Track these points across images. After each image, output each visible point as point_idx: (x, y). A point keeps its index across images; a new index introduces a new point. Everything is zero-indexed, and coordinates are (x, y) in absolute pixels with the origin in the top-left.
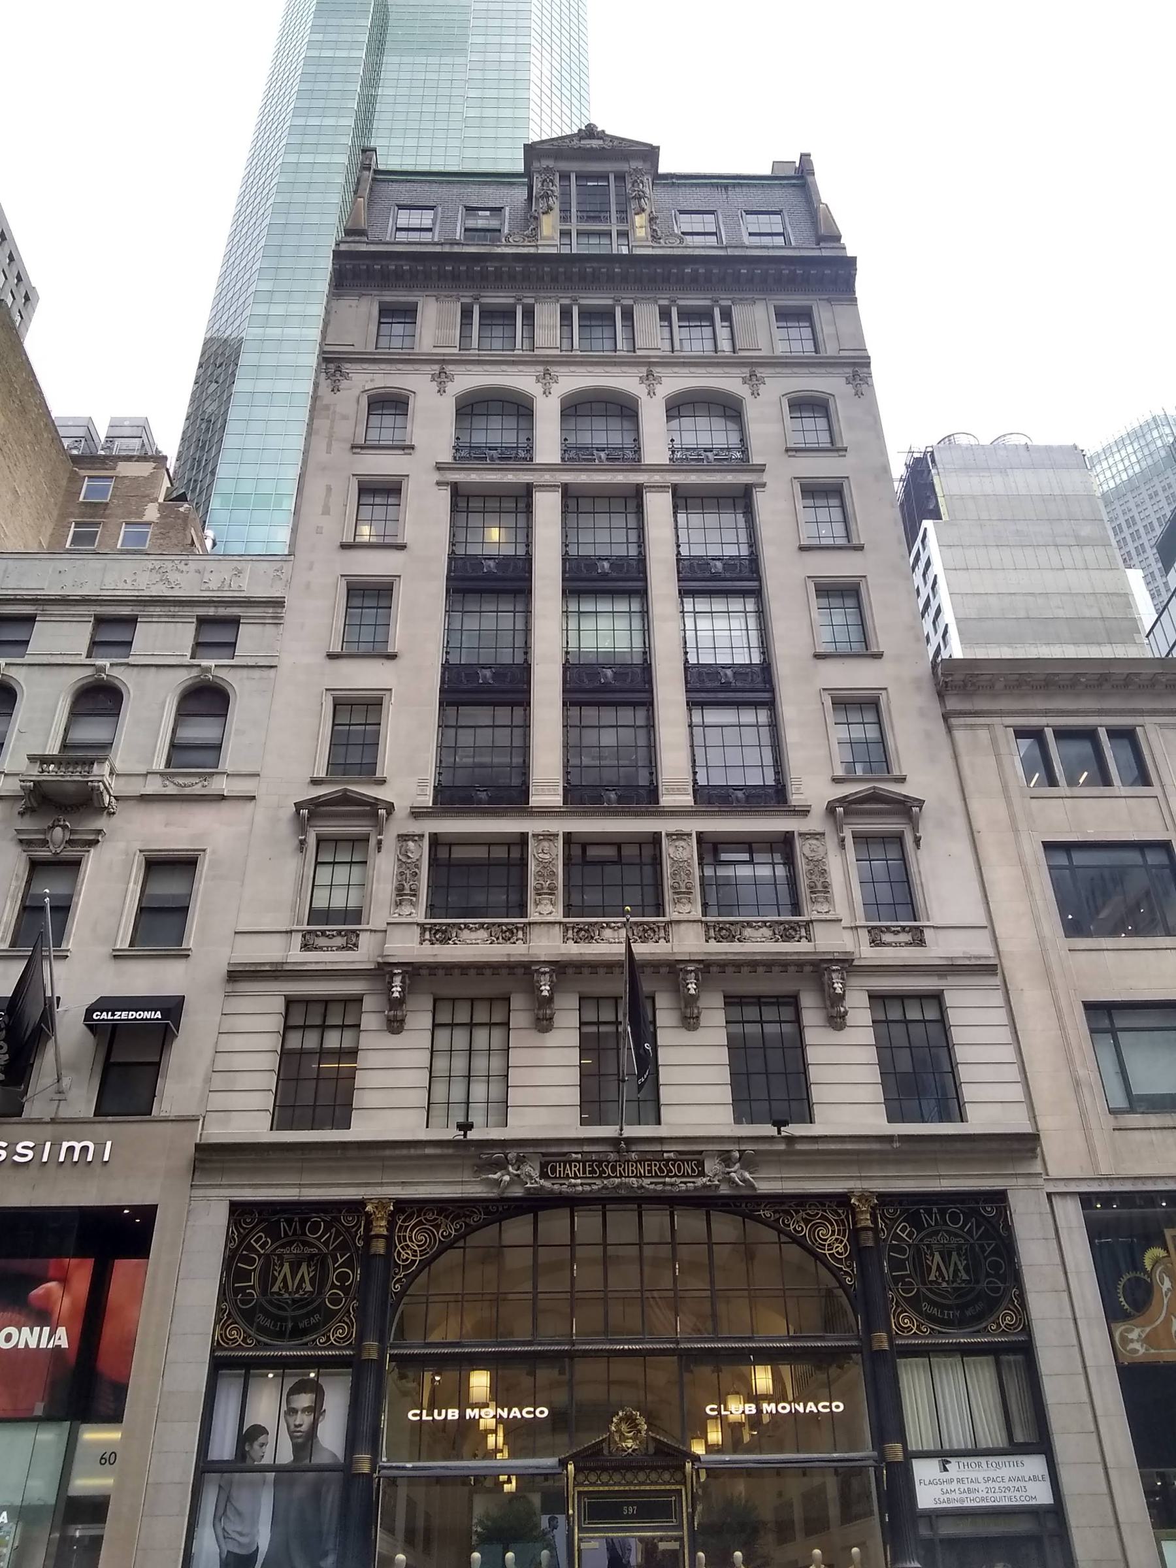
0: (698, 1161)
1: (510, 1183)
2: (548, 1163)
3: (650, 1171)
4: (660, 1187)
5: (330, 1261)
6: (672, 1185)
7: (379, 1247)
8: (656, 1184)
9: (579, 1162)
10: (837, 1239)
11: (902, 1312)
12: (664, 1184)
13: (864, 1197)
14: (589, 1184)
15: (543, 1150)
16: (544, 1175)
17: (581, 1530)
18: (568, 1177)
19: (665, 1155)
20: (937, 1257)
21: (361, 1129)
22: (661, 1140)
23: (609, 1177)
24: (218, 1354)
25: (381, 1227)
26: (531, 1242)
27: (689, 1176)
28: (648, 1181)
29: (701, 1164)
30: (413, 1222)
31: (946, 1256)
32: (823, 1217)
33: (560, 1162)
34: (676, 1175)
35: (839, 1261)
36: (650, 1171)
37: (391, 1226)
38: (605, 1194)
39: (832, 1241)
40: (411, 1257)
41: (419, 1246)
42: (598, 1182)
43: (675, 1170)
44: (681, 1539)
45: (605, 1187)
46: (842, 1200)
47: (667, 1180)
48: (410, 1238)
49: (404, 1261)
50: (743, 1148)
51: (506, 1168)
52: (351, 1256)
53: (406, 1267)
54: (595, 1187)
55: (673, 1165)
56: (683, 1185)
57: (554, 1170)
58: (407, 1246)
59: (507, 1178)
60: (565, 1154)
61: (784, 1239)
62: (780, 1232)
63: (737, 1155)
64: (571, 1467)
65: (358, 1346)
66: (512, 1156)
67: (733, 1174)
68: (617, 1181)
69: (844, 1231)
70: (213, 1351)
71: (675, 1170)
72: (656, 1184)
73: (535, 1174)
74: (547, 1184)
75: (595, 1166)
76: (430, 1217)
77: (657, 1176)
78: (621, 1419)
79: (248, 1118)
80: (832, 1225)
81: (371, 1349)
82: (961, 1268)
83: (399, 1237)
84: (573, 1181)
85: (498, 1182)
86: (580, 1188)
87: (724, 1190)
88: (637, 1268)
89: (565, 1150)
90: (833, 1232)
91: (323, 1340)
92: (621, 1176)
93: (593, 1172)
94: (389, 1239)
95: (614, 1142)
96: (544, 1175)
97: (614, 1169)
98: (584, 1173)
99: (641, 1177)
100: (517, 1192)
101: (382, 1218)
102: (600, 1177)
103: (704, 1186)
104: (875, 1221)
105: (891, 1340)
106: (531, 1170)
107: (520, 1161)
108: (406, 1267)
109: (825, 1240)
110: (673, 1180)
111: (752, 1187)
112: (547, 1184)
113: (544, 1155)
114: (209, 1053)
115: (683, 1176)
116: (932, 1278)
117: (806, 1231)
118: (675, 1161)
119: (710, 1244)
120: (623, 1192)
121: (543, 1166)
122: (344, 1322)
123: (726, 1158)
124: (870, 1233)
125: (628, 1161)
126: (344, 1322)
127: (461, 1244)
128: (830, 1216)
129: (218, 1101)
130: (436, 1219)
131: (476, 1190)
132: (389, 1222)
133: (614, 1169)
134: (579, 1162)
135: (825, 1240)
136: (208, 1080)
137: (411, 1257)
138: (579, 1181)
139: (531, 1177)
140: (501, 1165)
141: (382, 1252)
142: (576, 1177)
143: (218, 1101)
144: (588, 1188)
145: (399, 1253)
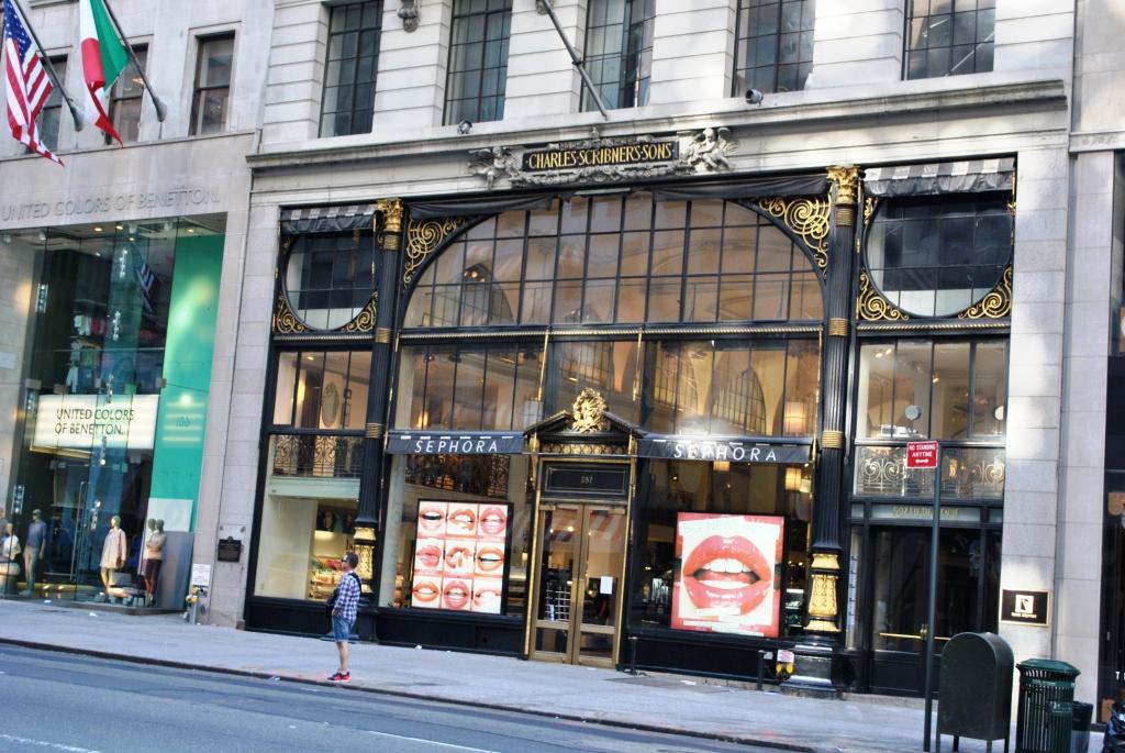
0: (673, 143)
2: (530, 154)
3: (624, 157)
4: (632, 174)
6: (644, 169)
8: (630, 169)
9: (557, 151)
10: (816, 219)
11: (873, 296)
12: (637, 169)
14: (567, 174)
16: (526, 168)
17: (543, 494)
18: (547, 169)
19: (639, 139)
21: (383, 131)
22: (632, 123)
23: (585, 165)
24: (276, 338)
25: (394, 224)
26: (649, 227)
27: (662, 160)
28: (622, 167)
29: (675, 146)
33: (540, 153)
34: (649, 160)
35: (815, 242)
36: (624, 157)
40: (420, 251)
41: (426, 241)
42: (574, 171)
43: (649, 155)
44: (626, 507)
45: (581, 177)
47: (639, 165)
48: (420, 233)
49: (415, 255)
51: (493, 163)
53: (416, 261)
54: (572, 177)
55: (647, 150)
56: (654, 170)
57: (534, 161)
59: (491, 173)
60: (545, 145)
61: (763, 220)
62: (759, 214)
64: (534, 442)
65: (373, 332)
67: (705, 156)
68: (591, 170)
69: (827, 208)
70: (272, 335)
71: (649, 155)
72: (630, 169)
73: (519, 165)
74: (528, 176)
75: (574, 153)
77: (631, 162)
78: (584, 398)
79: (297, 131)
81: (383, 337)
83: (411, 233)
84: (550, 172)
85: (484, 177)
86: (557, 179)
87: (701, 170)
88: (753, 254)
91: (352, 326)
92: (597, 163)
93: (571, 161)
95: (590, 127)
96: (526, 168)
97: (590, 157)
98: (562, 162)
99: (615, 163)
100: (504, 185)
101: (392, 216)
102: (576, 166)
103: (677, 169)
105: (849, 327)
107: (506, 152)
108: (416, 261)
109: (805, 220)
110: (644, 165)
111: (726, 165)
112: (528, 176)
114: (264, 65)
115: (656, 160)
117: (785, 211)
118: (649, 144)
119: (688, 230)
120: (599, 180)
121: (526, 157)
123: (699, 135)
125: (604, 148)
127: (463, 238)
129: (272, 113)
131: (472, 186)
132: (402, 220)
133: (590, 157)
134: (557, 151)
135: (805, 220)
136: (264, 95)
137: (420, 251)
138: (556, 172)
139: (512, 169)
140: (488, 158)
141: (393, 247)
142: (554, 168)
143: (272, 113)
144: (565, 179)
145: (411, 248)
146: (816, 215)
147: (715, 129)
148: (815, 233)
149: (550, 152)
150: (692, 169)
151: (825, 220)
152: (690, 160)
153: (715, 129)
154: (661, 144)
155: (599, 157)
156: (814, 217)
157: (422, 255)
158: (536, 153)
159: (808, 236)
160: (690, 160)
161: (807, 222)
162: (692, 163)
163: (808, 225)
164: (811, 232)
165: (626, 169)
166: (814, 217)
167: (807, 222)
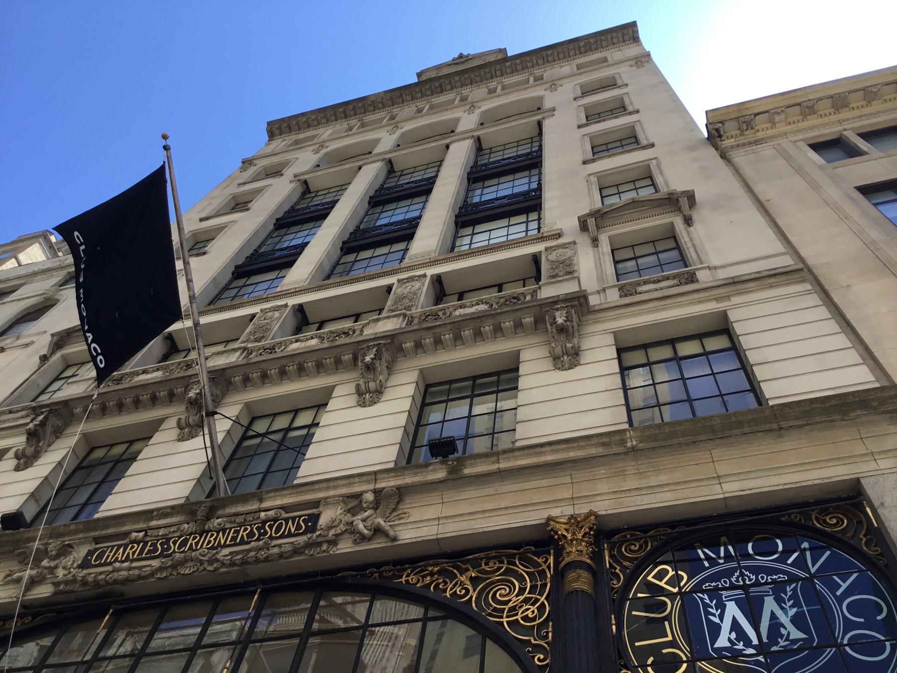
10: (526, 601)
13: (574, 521)
20: (732, 610)
31: (752, 609)
32: (508, 572)
39: (519, 602)
46: (542, 541)
50: (380, 485)
55: (271, 527)
63: (370, 497)
69: (545, 585)
80: (521, 579)
82: (784, 619)
90: (522, 591)
104: (597, 556)
113: (97, 540)
116: (722, 642)
123: (354, 503)
124: (585, 575)
128: (521, 570)
146: (526, 595)
147: (376, 492)
148: (526, 619)
151: (543, 599)
152: (332, 532)
153: (376, 492)
154: (293, 519)
156: (522, 598)
159: (513, 624)
160: (332, 532)
161: (511, 604)
162: (336, 535)
163: (510, 610)
164: (519, 617)
165: (231, 553)
166: (522, 598)
167: (511, 604)
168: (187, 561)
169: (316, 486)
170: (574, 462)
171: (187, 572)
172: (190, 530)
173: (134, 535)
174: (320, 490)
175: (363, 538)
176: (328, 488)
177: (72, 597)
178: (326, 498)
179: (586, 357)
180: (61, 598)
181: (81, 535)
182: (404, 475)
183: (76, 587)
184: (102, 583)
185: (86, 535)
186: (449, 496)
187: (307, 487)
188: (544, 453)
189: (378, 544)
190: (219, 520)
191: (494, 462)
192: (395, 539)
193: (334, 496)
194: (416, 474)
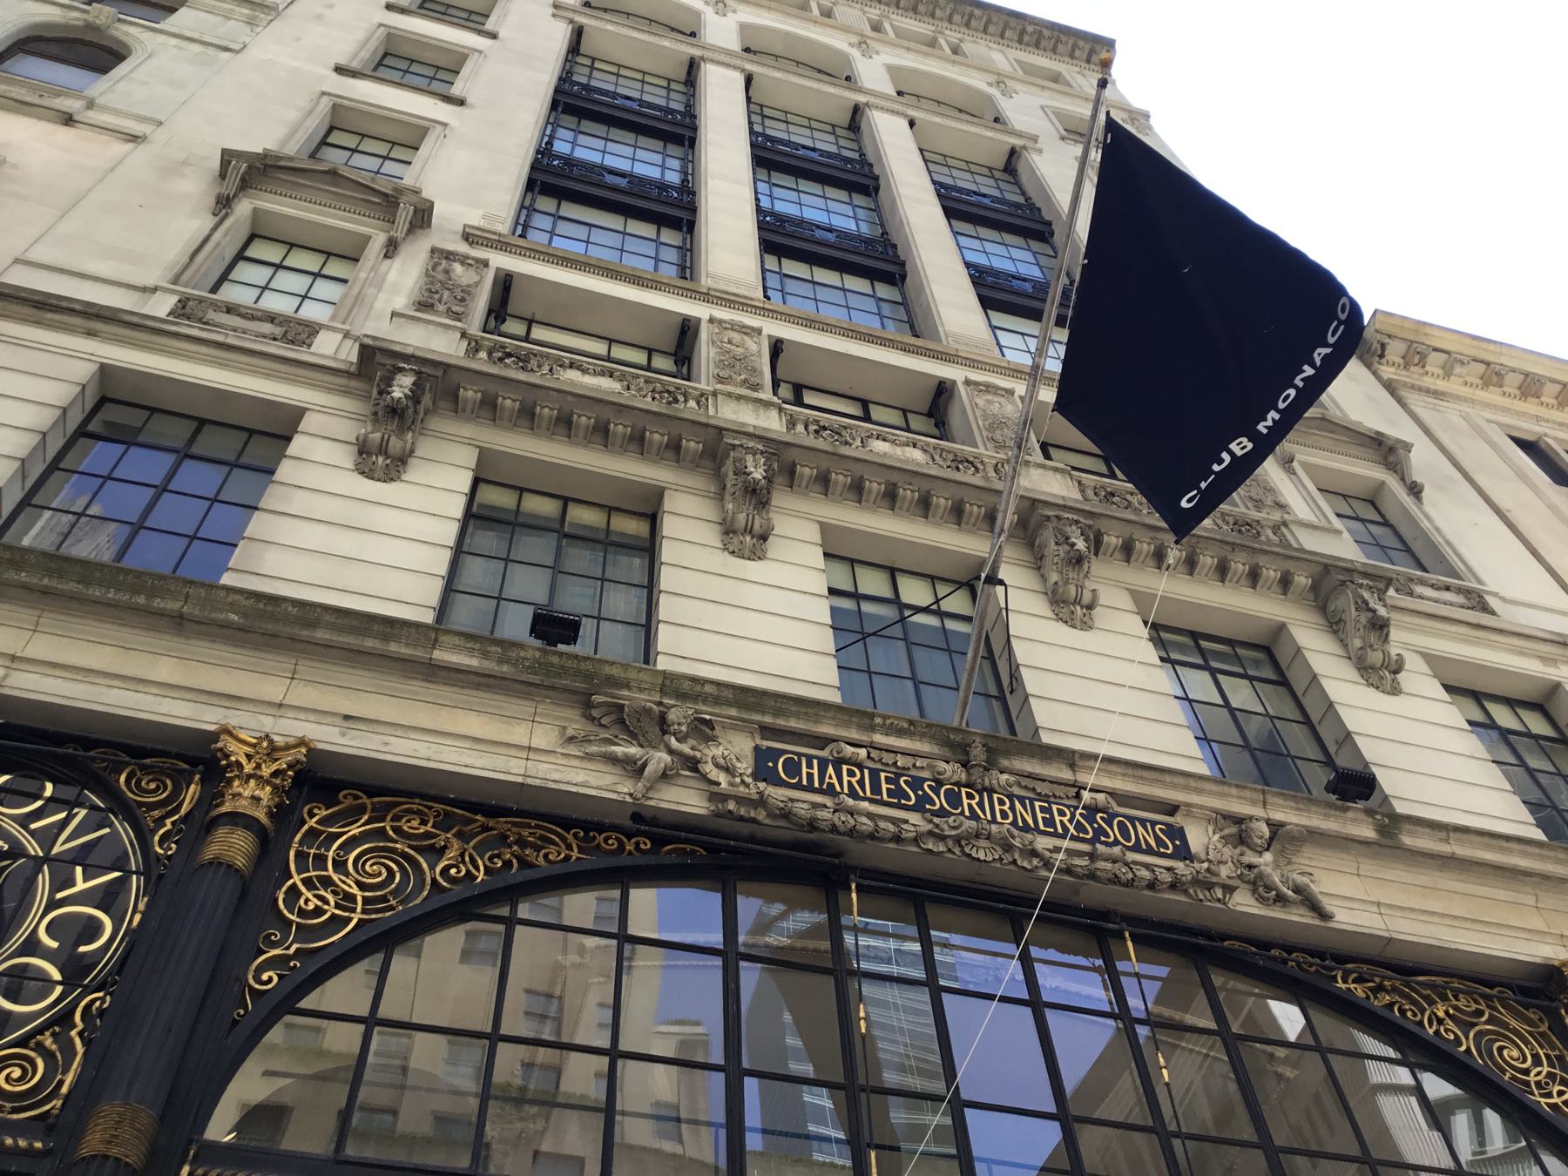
1: (665, 776)
5: (44, 880)
7: (234, 846)
9: (860, 766)
15: (768, 719)
16: (763, 772)
30: (355, 831)
33: (810, 758)
37: (286, 817)
38: (924, 868)
48: (340, 865)
49: (302, 913)
52: (122, 883)
53: (304, 932)
58: (327, 882)
60: (823, 741)
66: (679, 714)
76: (412, 825)
83: (299, 854)
89: (827, 729)
94: (269, 842)
98: (876, 789)
100: (686, 800)
106: (738, 747)
113: (766, 731)
122: (40, 1049)
125: (991, 791)
126: (40, 1049)
130: (428, 835)
137: (331, 910)
145: (294, 893)
149: (838, 763)
150: (1229, 889)
155: (981, 804)
157: (337, 922)
158: (800, 755)
168: (977, 836)
169: (1168, 778)
170: (1546, 877)
171: (981, 855)
172: (955, 778)
173: (849, 750)
174: (1175, 786)
175: (1280, 899)
176: (1186, 788)
177: (746, 829)
178: (1188, 805)
179: (774, 546)
180: (726, 825)
181: (733, 712)
182: (1309, 811)
183: (761, 815)
184: (823, 825)
185: (745, 716)
186: (1369, 867)
187: (1153, 775)
188: (1510, 851)
189: (1298, 916)
190: (1005, 777)
191: (1441, 840)
192: (1325, 916)
193: (1202, 807)
194: (1327, 816)
